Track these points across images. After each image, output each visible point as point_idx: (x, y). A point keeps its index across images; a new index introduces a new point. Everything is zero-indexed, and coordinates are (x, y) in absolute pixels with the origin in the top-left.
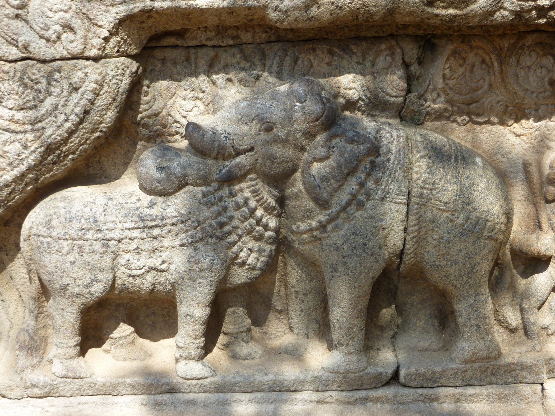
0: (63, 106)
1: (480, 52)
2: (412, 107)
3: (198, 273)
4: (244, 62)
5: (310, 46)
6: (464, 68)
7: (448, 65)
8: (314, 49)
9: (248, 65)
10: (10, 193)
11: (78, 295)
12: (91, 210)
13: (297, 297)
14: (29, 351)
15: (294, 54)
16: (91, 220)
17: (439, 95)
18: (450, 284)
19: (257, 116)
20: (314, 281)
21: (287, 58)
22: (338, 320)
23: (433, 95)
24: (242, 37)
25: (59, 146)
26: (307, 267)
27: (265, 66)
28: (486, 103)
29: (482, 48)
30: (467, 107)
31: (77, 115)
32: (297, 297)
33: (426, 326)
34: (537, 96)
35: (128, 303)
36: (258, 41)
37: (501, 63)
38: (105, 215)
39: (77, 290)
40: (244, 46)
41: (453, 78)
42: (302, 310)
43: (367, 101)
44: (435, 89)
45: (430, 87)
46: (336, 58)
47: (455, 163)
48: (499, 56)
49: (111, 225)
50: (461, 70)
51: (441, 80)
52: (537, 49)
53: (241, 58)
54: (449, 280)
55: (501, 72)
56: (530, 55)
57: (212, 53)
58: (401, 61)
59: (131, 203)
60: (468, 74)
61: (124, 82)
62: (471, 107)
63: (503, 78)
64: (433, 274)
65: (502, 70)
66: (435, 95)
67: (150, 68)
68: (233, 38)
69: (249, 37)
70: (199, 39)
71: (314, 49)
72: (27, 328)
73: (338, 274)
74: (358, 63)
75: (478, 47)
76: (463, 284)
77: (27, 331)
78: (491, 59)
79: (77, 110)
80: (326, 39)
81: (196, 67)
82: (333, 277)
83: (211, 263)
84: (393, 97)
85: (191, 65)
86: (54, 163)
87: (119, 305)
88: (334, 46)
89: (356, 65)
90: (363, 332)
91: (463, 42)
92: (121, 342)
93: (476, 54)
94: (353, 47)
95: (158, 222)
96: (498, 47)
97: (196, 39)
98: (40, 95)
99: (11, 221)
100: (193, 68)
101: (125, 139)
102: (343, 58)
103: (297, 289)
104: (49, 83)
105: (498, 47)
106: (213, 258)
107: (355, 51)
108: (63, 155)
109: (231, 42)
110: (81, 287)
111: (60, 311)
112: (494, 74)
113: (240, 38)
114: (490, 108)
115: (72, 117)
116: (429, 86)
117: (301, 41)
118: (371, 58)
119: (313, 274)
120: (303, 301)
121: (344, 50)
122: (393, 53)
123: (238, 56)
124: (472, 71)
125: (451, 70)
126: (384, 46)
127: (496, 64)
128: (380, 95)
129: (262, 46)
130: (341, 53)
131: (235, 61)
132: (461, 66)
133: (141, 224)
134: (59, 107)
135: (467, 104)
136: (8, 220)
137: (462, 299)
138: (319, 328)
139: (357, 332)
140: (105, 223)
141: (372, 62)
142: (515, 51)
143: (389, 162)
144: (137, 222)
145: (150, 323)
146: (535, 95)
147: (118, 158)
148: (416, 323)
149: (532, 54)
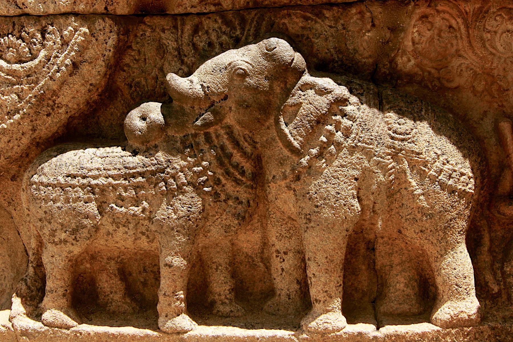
0: (55, 57)
1: (447, 16)
2: (383, 70)
3: (176, 221)
4: (224, 27)
5: (286, 12)
6: (432, 32)
7: (416, 29)
8: (289, 15)
9: (229, 29)
10: (9, 141)
11: (65, 241)
12: (79, 158)
13: (277, 256)
14: (24, 299)
15: (271, 18)
16: (78, 166)
17: (409, 60)
18: (426, 239)
19: (230, 64)
20: (294, 238)
21: (264, 23)
22: (314, 274)
23: (403, 58)
24: (223, 4)
25: (52, 97)
26: (286, 224)
27: (244, 30)
28: (456, 67)
29: (448, 13)
30: (437, 71)
31: (67, 66)
32: (277, 256)
33: (405, 289)
34: (505, 61)
35: (119, 257)
36: (237, 7)
37: (467, 27)
38: (92, 162)
39: (63, 236)
40: (226, 12)
41: (421, 41)
42: (283, 270)
43: (340, 63)
44: (404, 52)
45: (400, 51)
46: (309, 21)
47: (425, 114)
48: (465, 20)
49: (97, 172)
50: (428, 34)
51: (411, 44)
52: (503, 14)
53: (222, 22)
54: (425, 235)
55: (468, 36)
56: (495, 20)
57: (196, 20)
58: (371, 24)
59: (117, 152)
60: (436, 37)
61: (112, 37)
62: (441, 72)
63: (470, 42)
64: (409, 228)
65: (469, 34)
66: (405, 59)
67: (141, 33)
68: (215, 5)
69: (229, 3)
70: (184, 6)
71: (289, 15)
72: (25, 278)
73: (312, 224)
74: (331, 27)
75: (444, 12)
76: (440, 238)
77: (26, 280)
78: (458, 23)
79: (68, 61)
80: (300, 5)
81: (182, 32)
82: (307, 228)
83: (189, 211)
84: (364, 58)
85: (178, 31)
86: (48, 115)
87: (111, 258)
88: (308, 12)
89: (328, 28)
90: (341, 289)
91: (429, 6)
92: (111, 296)
93: (443, 19)
94: (325, 12)
95: (139, 170)
96: (464, 11)
97: (182, 6)
98: (34, 46)
99: (18, 176)
100: (179, 33)
101: (120, 102)
102: (316, 22)
103: (278, 247)
104: (44, 37)
105: (464, 11)
106: (190, 206)
107: (327, 15)
108: (56, 105)
109: (213, 8)
110: (67, 232)
111: (50, 259)
112: (461, 37)
113: (221, 5)
114: (460, 74)
115: (63, 68)
116: (398, 50)
117: (276, 7)
118: (342, 21)
119: (291, 231)
120: (284, 260)
121: (317, 15)
122: (363, 17)
123: (220, 21)
124: (439, 35)
125: (419, 34)
126: (354, 11)
127: (462, 27)
128: (351, 56)
129: (241, 12)
130: (314, 18)
131: (216, 26)
132: (429, 30)
133: (124, 171)
134: (52, 59)
135: (436, 69)
136: (15, 175)
137: (439, 257)
138: (300, 288)
139: (334, 289)
140: (90, 170)
141: (343, 25)
142: (481, 15)
143: (359, 111)
144: (119, 169)
145: (142, 280)
146: (503, 60)
147: (114, 119)
148: (396, 286)
149: (498, 18)
